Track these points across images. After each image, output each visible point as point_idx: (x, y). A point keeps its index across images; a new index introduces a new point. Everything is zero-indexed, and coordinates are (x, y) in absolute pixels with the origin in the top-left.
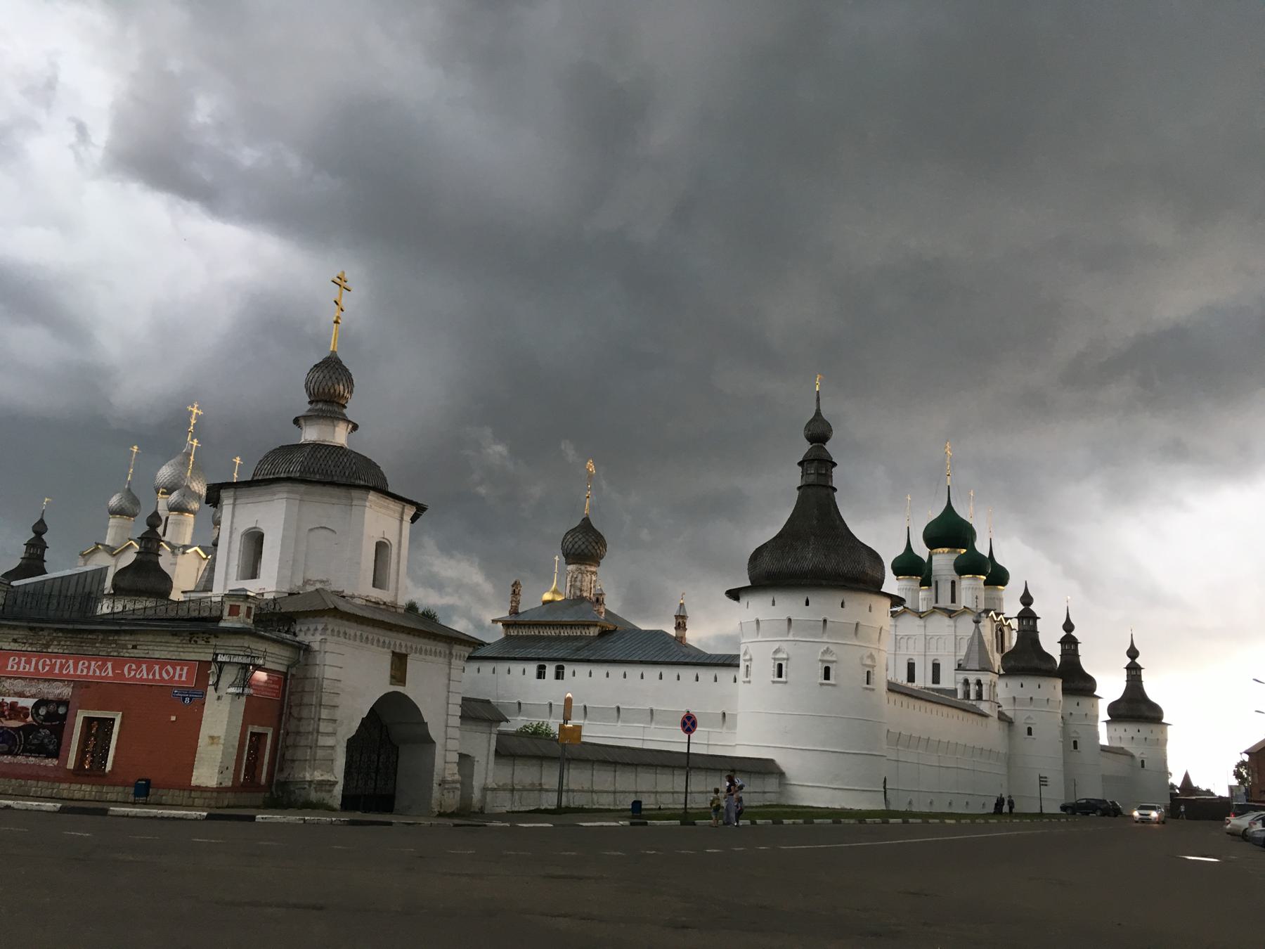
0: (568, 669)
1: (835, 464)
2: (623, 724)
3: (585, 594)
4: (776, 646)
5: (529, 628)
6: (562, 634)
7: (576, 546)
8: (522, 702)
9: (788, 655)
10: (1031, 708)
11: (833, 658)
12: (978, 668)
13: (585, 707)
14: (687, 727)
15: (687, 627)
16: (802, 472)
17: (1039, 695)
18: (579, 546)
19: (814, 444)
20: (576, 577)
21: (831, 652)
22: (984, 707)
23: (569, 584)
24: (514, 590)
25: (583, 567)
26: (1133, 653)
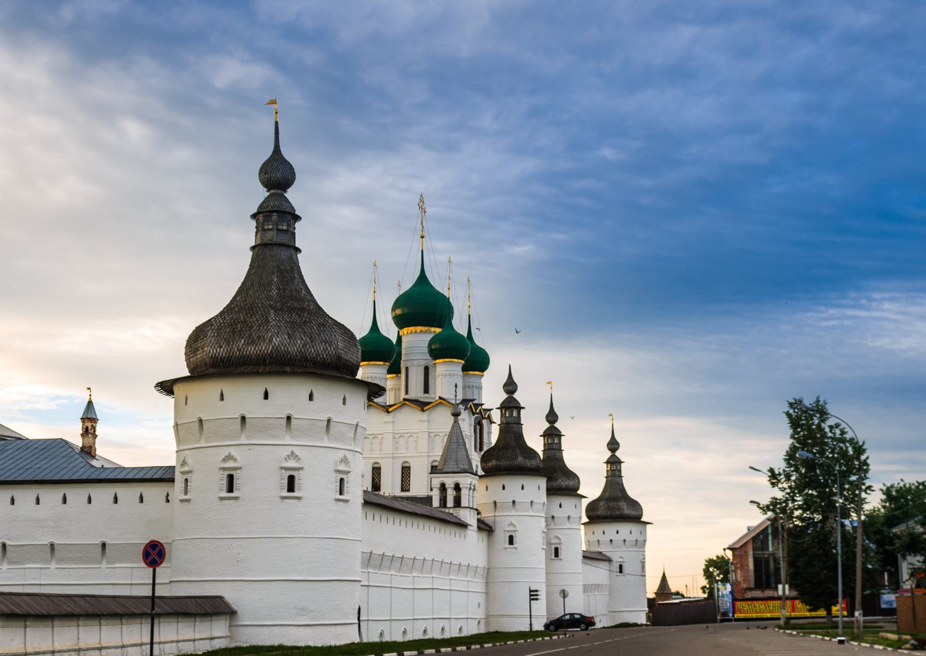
1: (297, 218)
2: (57, 567)
4: (225, 452)
10: (513, 513)
12: (456, 470)
14: (150, 559)
15: (97, 433)
16: (257, 228)
17: (522, 497)
19: (272, 191)
26: (613, 445)
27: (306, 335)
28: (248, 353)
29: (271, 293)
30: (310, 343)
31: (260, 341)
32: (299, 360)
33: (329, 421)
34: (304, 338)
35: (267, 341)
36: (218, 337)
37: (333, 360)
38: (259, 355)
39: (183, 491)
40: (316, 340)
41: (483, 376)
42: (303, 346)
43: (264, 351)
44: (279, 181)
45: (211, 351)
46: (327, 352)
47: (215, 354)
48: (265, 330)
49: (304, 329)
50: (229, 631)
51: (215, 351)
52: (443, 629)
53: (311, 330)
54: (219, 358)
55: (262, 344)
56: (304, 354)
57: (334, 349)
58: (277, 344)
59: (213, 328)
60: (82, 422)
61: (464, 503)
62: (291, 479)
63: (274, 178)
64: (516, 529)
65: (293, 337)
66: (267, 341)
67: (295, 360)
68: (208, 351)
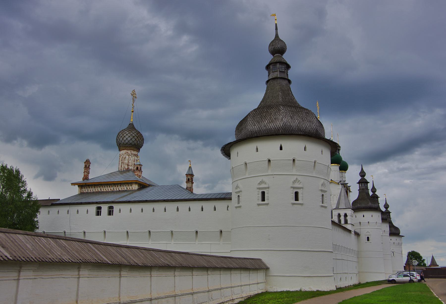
0: (116, 207)
3: (130, 168)
4: (260, 179)
5: (95, 187)
6: (115, 190)
7: (125, 139)
8: (86, 231)
9: (268, 185)
11: (300, 186)
12: (345, 208)
13: (127, 232)
15: (193, 181)
18: (127, 139)
20: (125, 158)
22: (349, 227)
23: (120, 163)
24: (86, 165)
25: (129, 152)
27: (300, 117)
28: (270, 127)
29: (279, 100)
30: (302, 122)
32: (297, 130)
34: (299, 119)
41: (346, 173)
44: (279, 49)
45: (250, 128)
55: (277, 122)
56: (299, 128)
58: (285, 122)
59: (250, 116)
60: (186, 176)
61: (349, 222)
64: (370, 234)
65: (293, 119)
67: (295, 130)
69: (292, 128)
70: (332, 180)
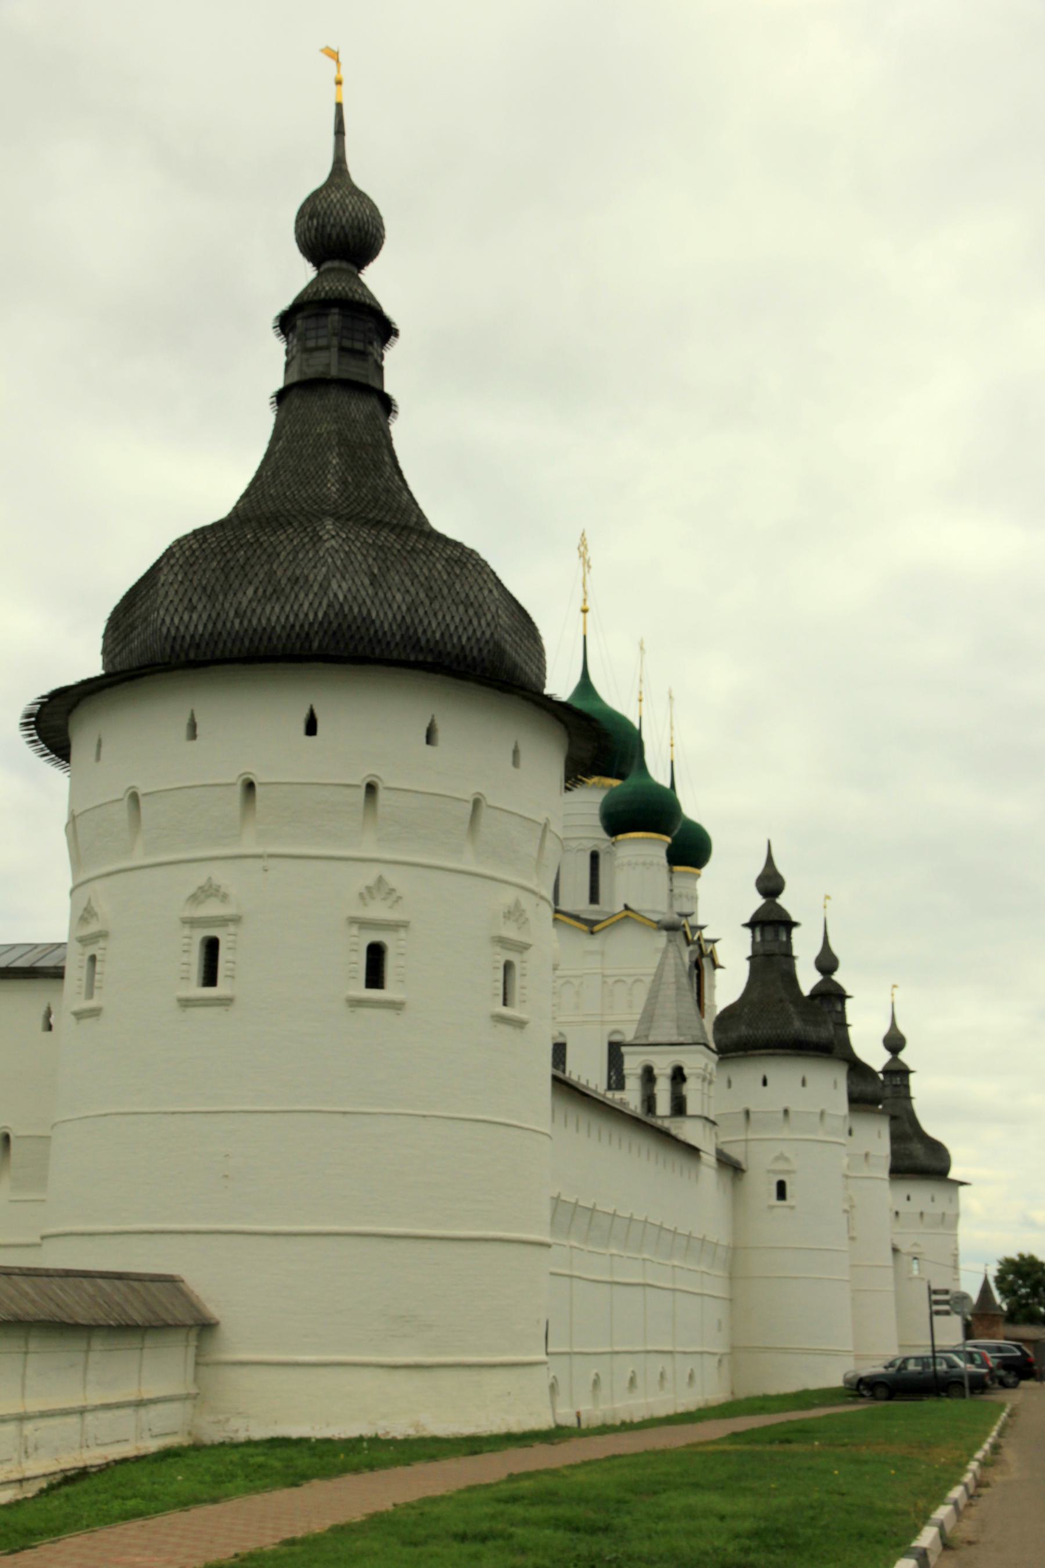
4: (198, 877)
10: (786, 1134)
12: (675, 1039)
16: (287, 352)
21: (393, 890)
22: (689, 1131)
27: (416, 581)
28: (264, 622)
29: (325, 490)
30: (427, 602)
31: (296, 589)
32: (397, 644)
33: (477, 803)
34: (412, 590)
35: (316, 588)
36: (187, 583)
37: (485, 651)
38: (293, 626)
39: (83, 990)
40: (443, 597)
41: (699, 876)
42: (409, 609)
43: (306, 615)
44: (346, 236)
45: (168, 620)
46: (470, 631)
47: (177, 628)
48: (310, 560)
49: (411, 567)
50: (196, 1379)
51: (176, 621)
52: (662, 1375)
53: (430, 570)
54: (188, 638)
55: (302, 595)
56: (411, 631)
57: (488, 625)
58: (341, 598)
59: (172, 561)
61: (693, 1106)
62: (376, 955)
63: (333, 226)
65: (384, 584)
66: (316, 588)
67: (388, 643)
68: (159, 621)
69: (376, 632)
70: (631, 905)
